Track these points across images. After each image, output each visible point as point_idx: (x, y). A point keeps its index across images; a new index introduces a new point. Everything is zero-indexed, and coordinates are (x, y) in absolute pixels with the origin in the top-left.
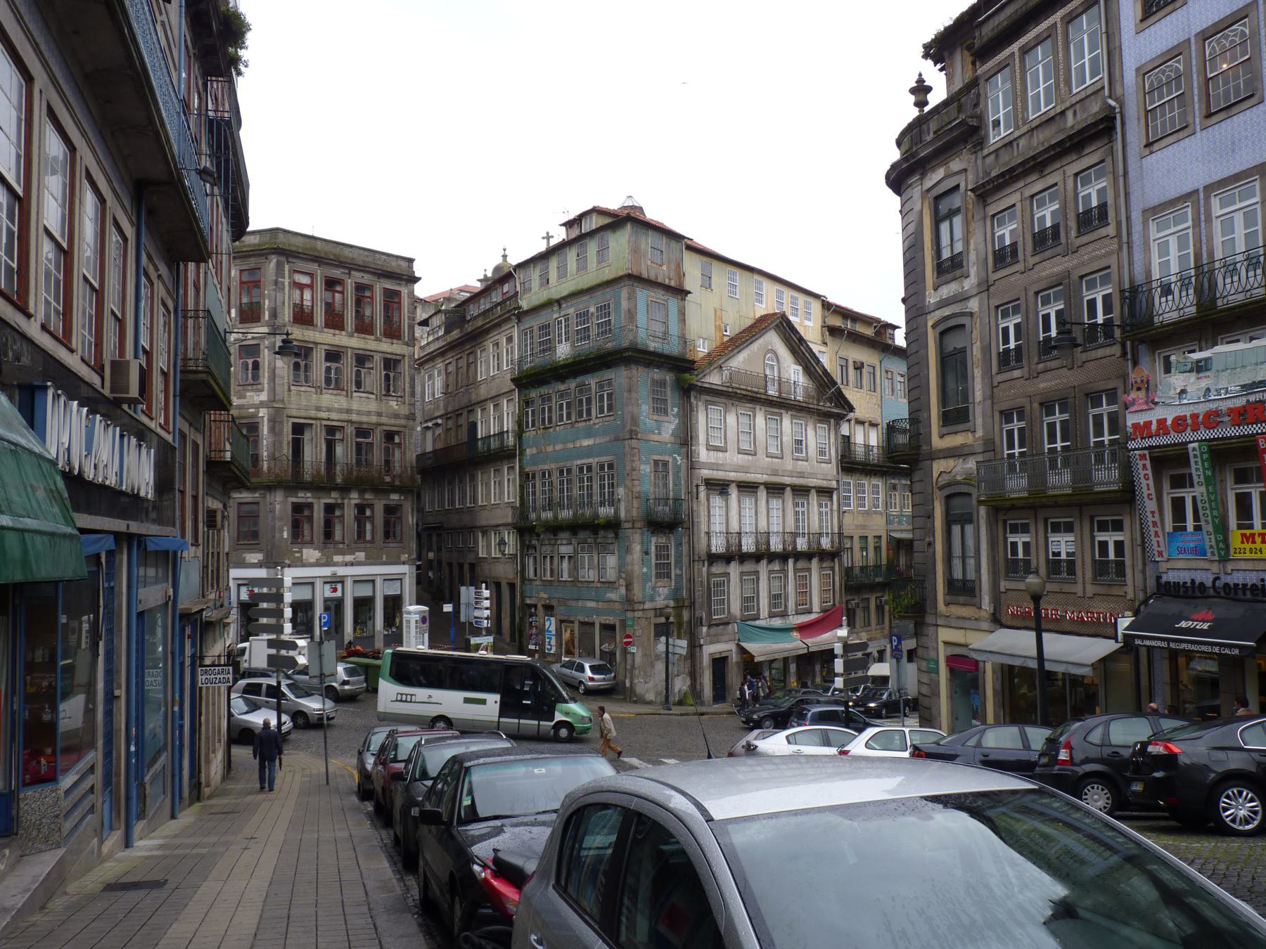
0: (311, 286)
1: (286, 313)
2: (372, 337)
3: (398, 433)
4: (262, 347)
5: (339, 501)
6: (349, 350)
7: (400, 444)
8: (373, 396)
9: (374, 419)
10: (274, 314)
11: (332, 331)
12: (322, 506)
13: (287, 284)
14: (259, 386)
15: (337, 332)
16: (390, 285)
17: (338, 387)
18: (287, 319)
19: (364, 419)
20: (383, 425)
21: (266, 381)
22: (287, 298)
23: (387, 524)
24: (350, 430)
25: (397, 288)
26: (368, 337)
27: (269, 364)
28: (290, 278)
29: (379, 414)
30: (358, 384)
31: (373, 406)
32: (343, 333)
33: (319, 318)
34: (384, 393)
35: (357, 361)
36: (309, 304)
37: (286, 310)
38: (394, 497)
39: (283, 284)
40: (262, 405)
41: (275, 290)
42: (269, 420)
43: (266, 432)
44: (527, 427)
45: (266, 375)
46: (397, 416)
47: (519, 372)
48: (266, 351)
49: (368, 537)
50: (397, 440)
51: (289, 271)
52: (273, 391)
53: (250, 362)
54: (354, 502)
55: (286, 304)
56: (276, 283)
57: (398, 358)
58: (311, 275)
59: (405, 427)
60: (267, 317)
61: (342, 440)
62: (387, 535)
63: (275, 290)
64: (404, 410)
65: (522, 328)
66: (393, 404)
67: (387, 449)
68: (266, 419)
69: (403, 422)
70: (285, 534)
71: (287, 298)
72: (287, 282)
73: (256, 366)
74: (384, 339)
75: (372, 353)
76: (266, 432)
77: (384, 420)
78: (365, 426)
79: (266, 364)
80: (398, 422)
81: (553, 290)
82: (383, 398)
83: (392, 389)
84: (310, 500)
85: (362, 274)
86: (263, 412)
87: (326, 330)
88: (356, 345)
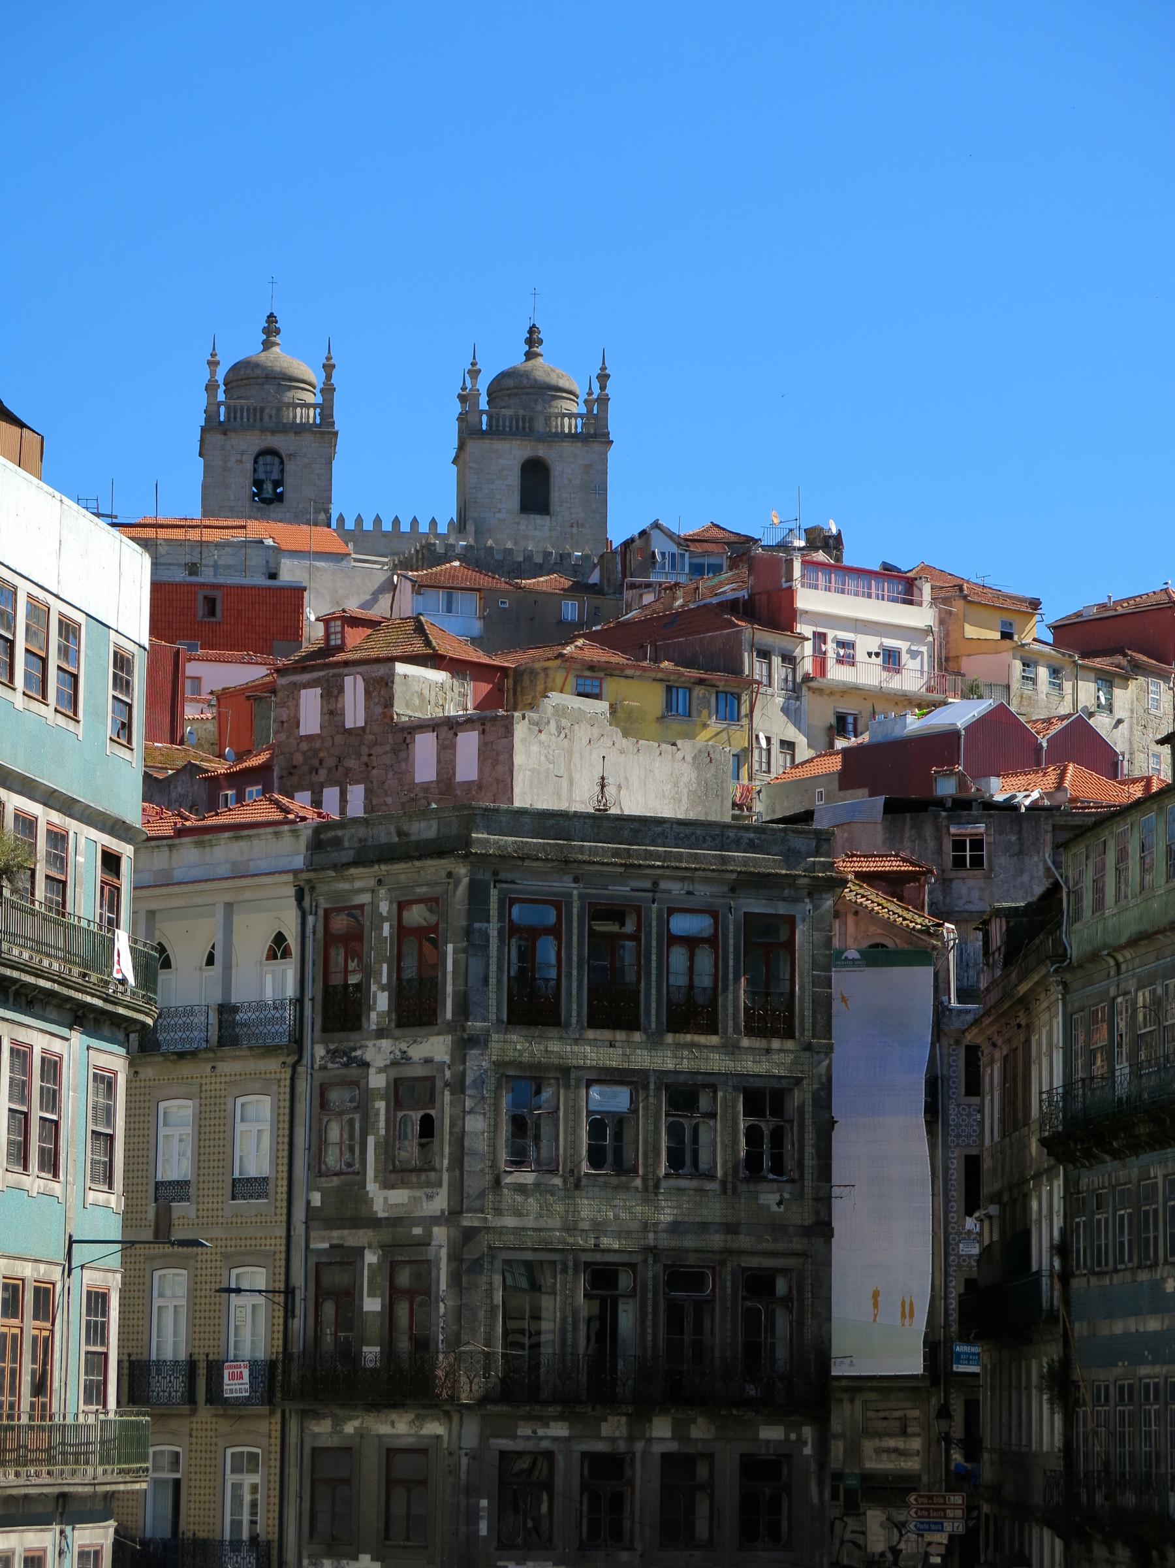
0: (555, 931)
1: (493, 1002)
2: (714, 1040)
3: (784, 1271)
4: (439, 1084)
5: (622, 1446)
6: (652, 1080)
7: (787, 1300)
8: (714, 1186)
9: (717, 1240)
10: (464, 1008)
11: (607, 1034)
12: (576, 1457)
13: (493, 933)
14: (433, 1175)
15: (620, 1035)
16: (756, 905)
17: (623, 1168)
18: (493, 1017)
19: (690, 1242)
20: (741, 1252)
21: (446, 1162)
22: (493, 967)
23: (748, 1503)
24: (651, 1271)
25: (782, 909)
26: (702, 1039)
27: (452, 1125)
28: (501, 918)
29: (731, 1228)
30: (676, 1160)
31: (714, 1210)
32: (637, 1036)
33: (575, 1002)
34: (742, 1173)
35: (672, 1103)
36: (553, 973)
37: (493, 996)
38: (771, 1433)
39: (486, 936)
40: (435, 1220)
41: (465, 951)
42: (451, 1258)
43: (443, 1286)
44: (1078, 1267)
45: (447, 1150)
46: (778, 1228)
47: (1065, 1121)
48: (447, 1093)
49: (702, 1530)
50: (781, 1286)
51: (501, 902)
52: (458, 1189)
53: (416, 1116)
54: (658, 1449)
55: (493, 981)
56: (468, 932)
57: (784, 1084)
58: (557, 906)
59: (803, 1255)
60: (449, 1016)
61: (632, 1294)
62: (749, 1534)
63: (465, 951)
64: (799, 1215)
65: (1069, 1009)
66: (769, 1198)
67: (752, 1319)
68: (444, 1253)
69: (797, 1244)
70: (483, 1528)
71: (493, 967)
72: (493, 929)
73: (428, 1127)
74: (745, 1042)
75: (712, 1080)
76: (443, 1286)
77: (744, 1241)
78: (691, 1260)
79: (447, 1122)
80: (781, 1246)
81: (1111, 923)
82: (743, 1187)
83: (767, 1163)
84: (545, 1444)
85: (687, 886)
86: (440, 1234)
87: (591, 1034)
88: (670, 1065)
